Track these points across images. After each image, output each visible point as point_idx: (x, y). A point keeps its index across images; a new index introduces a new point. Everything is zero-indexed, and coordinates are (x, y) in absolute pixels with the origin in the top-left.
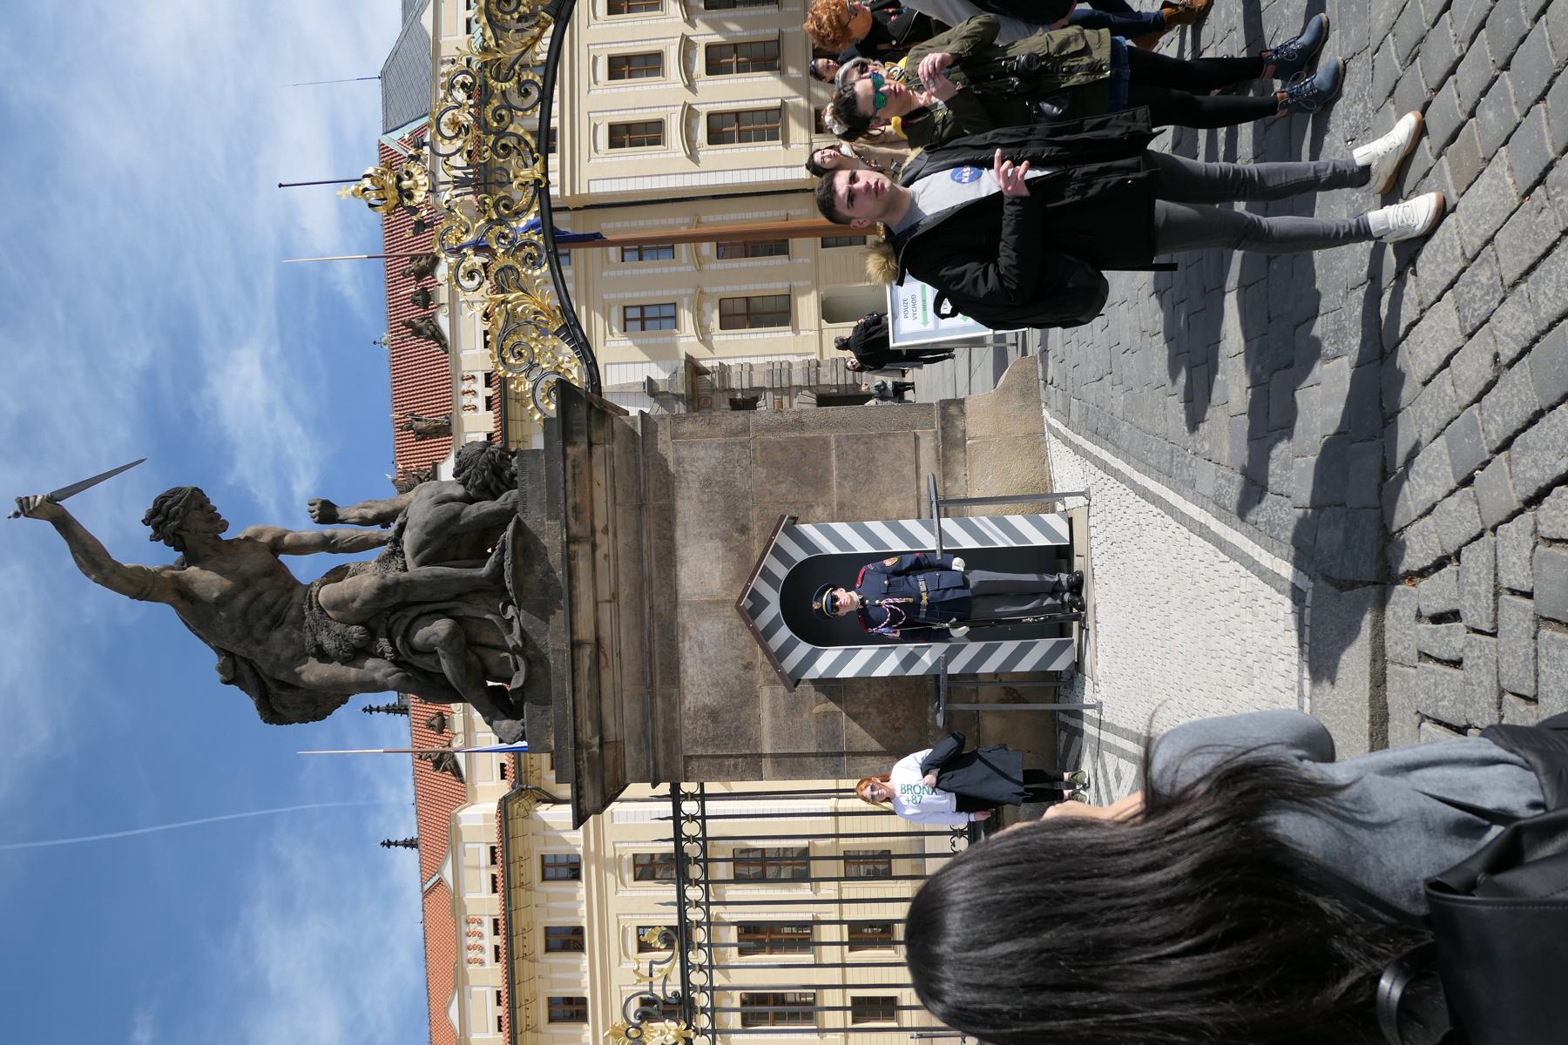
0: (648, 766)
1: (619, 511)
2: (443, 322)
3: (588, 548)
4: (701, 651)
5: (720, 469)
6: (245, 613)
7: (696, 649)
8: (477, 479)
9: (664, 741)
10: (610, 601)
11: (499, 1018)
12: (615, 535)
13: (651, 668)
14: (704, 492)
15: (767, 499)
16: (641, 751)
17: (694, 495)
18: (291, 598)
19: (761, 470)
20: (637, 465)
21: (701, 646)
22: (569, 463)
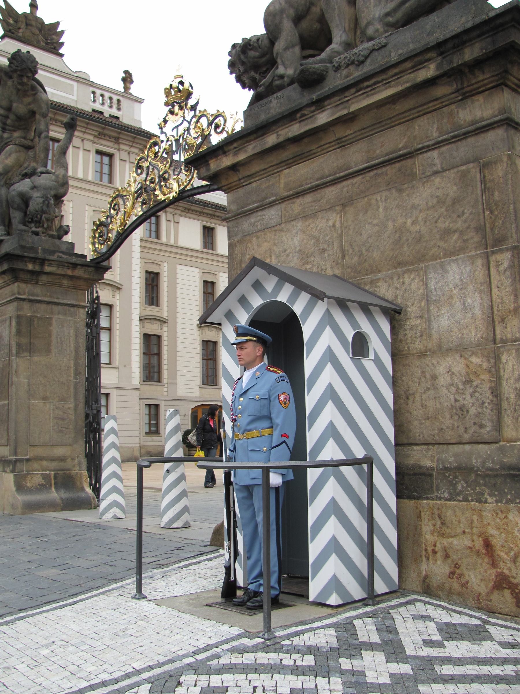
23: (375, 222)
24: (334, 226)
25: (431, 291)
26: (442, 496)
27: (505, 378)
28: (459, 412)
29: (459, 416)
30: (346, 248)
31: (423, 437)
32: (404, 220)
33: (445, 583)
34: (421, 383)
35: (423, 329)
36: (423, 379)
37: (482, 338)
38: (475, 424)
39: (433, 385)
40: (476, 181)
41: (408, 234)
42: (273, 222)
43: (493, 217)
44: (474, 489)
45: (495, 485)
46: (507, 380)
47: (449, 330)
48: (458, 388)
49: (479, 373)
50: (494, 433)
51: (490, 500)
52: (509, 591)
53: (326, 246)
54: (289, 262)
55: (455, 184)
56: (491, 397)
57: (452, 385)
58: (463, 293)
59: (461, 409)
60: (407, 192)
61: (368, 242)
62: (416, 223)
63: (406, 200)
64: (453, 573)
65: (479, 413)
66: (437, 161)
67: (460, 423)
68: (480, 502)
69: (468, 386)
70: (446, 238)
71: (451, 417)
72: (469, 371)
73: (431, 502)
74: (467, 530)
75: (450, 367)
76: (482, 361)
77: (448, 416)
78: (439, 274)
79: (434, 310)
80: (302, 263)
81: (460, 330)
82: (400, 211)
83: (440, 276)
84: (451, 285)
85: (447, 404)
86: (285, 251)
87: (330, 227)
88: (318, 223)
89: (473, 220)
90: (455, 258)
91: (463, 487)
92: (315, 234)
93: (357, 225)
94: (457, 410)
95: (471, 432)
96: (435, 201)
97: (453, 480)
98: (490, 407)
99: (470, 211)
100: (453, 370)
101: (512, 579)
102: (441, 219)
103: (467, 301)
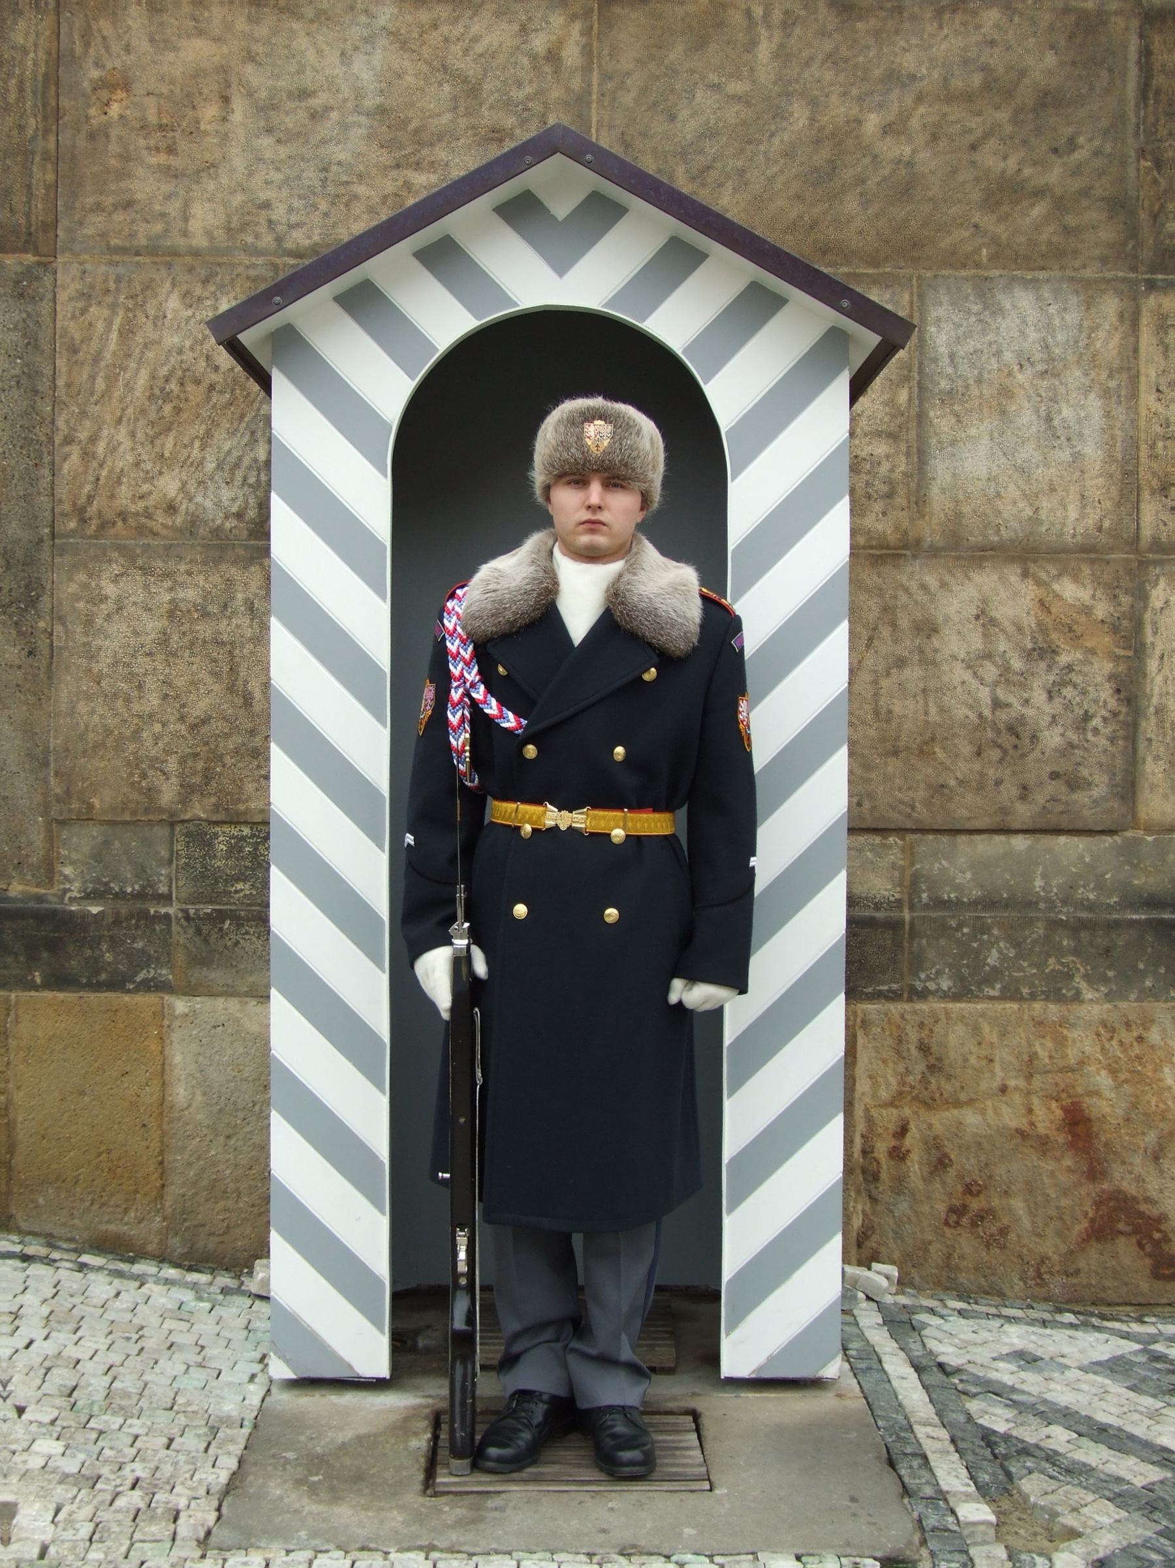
23: (736, 87)
24: (553, 56)
25: (935, 360)
26: (932, 986)
27: (1158, 653)
28: (1007, 740)
29: (1005, 752)
31: (874, 808)
32: (855, 111)
33: (930, 1243)
34: (876, 642)
35: (897, 475)
36: (885, 632)
37: (1100, 529)
38: (1054, 776)
39: (921, 651)
40: (1126, 59)
41: (867, 160)
44: (1040, 966)
45: (1107, 950)
46: (1162, 657)
47: (991, 492)
48: (1007, 668)
49: (1079, 630)
50: (1115, 804)
51: (1088, 995)
52: (1134, 1239)
54: (324, 142)
55: (1052, 47)
56: (1112, 703)
57: (988, 656)
58: (1048, 389)
59: (1012, 730)
60: (873, 22)
61: (701, 152)
62: (899, 133)
63: (868, 47)
64: (958, 1211)
65: (1071, 745)
67: (1008, 772)
68: (1060, 999)
69: (1043, 665)
70: (1005, 208)
71: (979, 754)
72: (1048, 621)
73: (895, 1008)
74: (1012, 1083)
75: (985, 601)
76: (1093, 597)
77: (966, 749)
78: (969, 312)
79: (941, 421)
80: (385, 158)
81: (1031, 498)
82: (841, 78)
83: (973, 319)
84: (1008, 356)
85: (965, 711)
86: (304, 94)
87: (534, 57)
88: (475, 29)
89: (1101, 173)
91: (1003, 957)
92: (468, 66)
93: (658, 78)
94: (999, 732)
95: (1040, 798)
96: (977, 80)
97: (974, 937)
98: (1108, 731)
99: (1097, 143)
100: (996, 614)
101: (1143, 1207)
102: (992, 143)
103: (1059, 412)
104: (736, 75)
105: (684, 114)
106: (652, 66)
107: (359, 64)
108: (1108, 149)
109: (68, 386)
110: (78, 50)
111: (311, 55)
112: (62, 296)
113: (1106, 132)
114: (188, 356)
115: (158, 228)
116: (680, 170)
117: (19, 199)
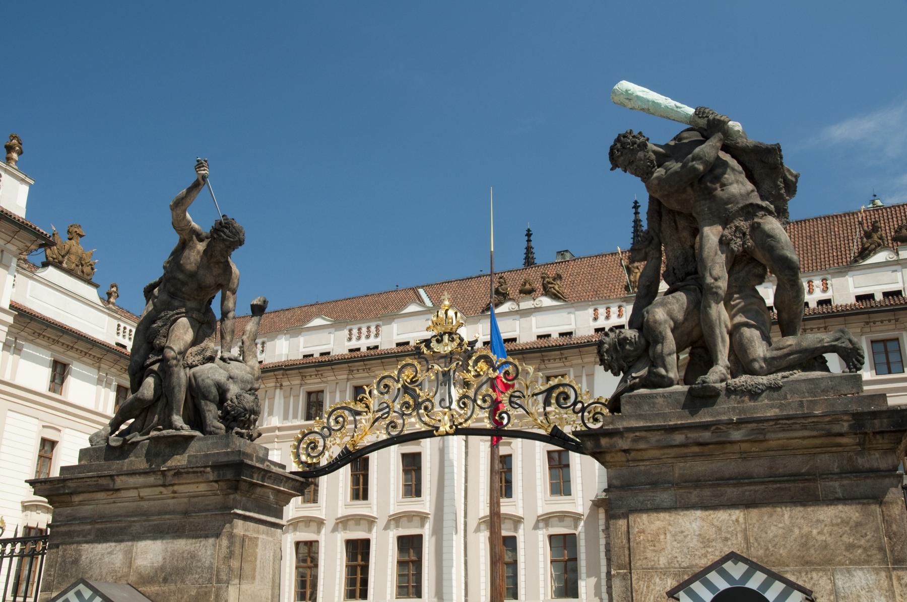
0: (59, 521)
1: (186, 500)
2: (881, 256)
3: (160, 482)
4: (109, 553)
5: (199, 564)
6: (175, 278)
7: (109, 550)
8: (230, 407)
9: (69, 531)
10: (139, 496)
11: (312, 355)
12: (174, 498)
13: (104, 522)
14: (188, 554)
15: (180, 596)
16: (67, 517)
17: (188, 547)
18: (189, 300)
19: (195, 591)
20: (208, 510)
21: (111, 553)
22: (202, 469)
23: (780, 525)
24: (737, 521)
25: (839, 589)
30: (751, 541)
32: (810, 529)
42: (665, 505)
43: (892, 543)
53: (729, 536)
66: (839, 490)
70: (851, 551)
80: (702, 546)
84: (858, 587)
86: (682, 532)
87: (733, 521)
90: (860, 567)
96: (839, 520)
102: (845, 535)
104: (780, 522)
105: (769, 532)
106: (760, 521)
107: (694, 525)
108: (876, 535)
109: (636, 599)
110: (633, 525)
111: (683, 524)
112: (633, 579)
113: (874, 532)
114: (662, 592)
115: (653, 563)
116: (770, 545)
117: (622, 558)
